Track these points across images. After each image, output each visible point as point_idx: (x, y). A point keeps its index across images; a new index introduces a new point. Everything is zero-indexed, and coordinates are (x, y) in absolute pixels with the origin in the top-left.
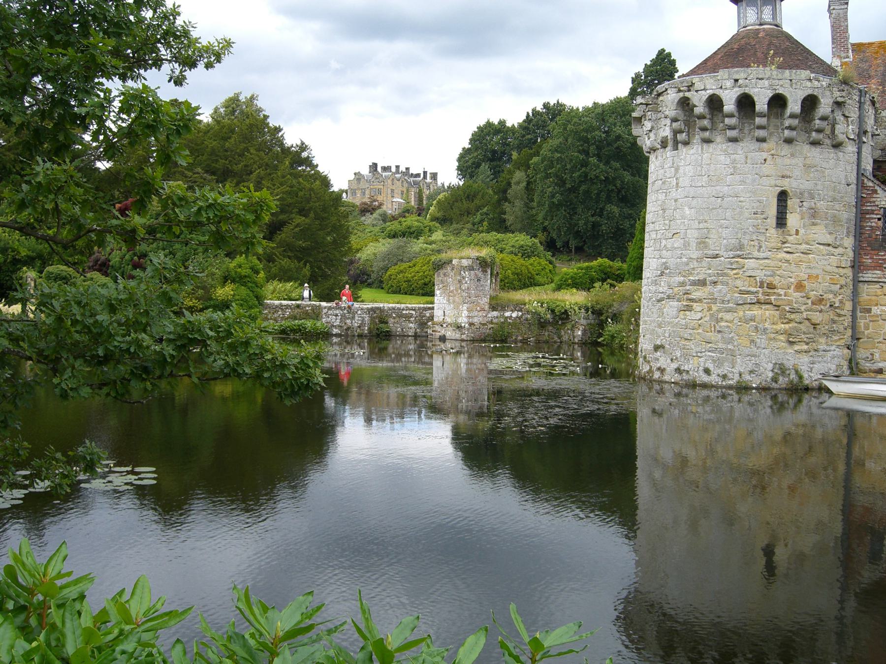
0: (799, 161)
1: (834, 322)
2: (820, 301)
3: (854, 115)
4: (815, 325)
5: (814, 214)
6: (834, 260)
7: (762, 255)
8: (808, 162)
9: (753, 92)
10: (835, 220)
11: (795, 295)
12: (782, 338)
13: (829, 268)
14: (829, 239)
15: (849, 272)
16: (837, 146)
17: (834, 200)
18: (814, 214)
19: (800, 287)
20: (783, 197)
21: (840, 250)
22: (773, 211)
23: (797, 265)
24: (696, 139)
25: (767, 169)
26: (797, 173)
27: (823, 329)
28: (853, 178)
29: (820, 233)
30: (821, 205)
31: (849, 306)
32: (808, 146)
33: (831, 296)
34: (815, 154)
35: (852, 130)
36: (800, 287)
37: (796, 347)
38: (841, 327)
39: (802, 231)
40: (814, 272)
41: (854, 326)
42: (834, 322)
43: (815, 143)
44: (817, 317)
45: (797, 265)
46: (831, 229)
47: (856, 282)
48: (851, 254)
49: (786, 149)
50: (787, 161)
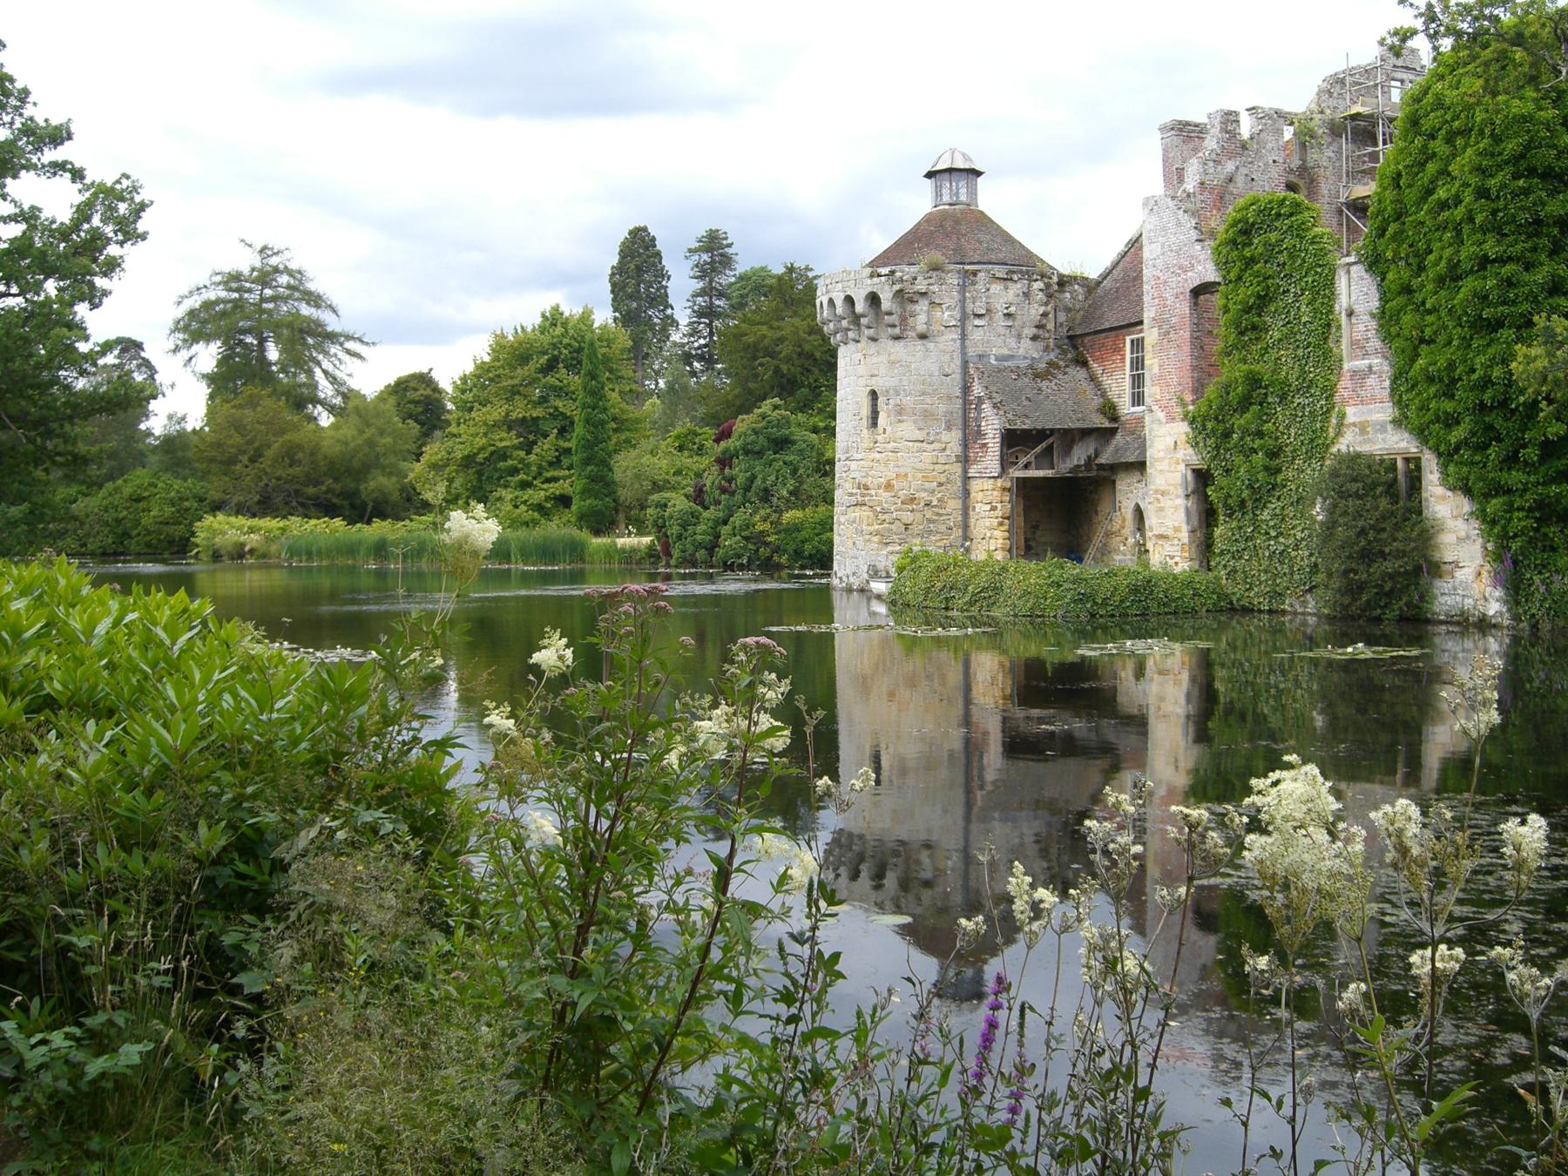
0: (883, 358)
1: (930, 521)
2: (913, 500)
3: (950, 298)
4: (907, 526)
5: (900, 411)
6: (927, 457)
7: (859, 456)
8: (892, 358)
9: (833, 295)
10: (927, 415)
11: (885, 495)
12: (876, 539)
13: (920, 466)
14: (919, 435)
15: (957, 469)
16: (923, 337)
17: (924, 394)
18: (900, 411)
19: (888, 486)
20: (874, 395)
21: (936, 446)
22: (865, 411)
23: (886, 465)
24: (864, 340)
25: (862, 370)
26: (883, 371)
27: (916, 529)
28: (955, 366)
29: (908, 430)
30: (908, 401)
31: (954, 505)
32: (891, 342)
33: (924, 495)
34: (898, 349)
35: (948, 316)
36: (888, 486)
37: (890, 548)
38: (942, 528)
39: (889, 429)
40: (902, 471)
41: (966, 526)
42: (934, 522)
43: (897, 338)
44: (907, 517)
45: (886, 465)
46: (921, 424)
47: (966, 479)
48: (958, 450)
49: (873, 347)
50: (875, 360)
